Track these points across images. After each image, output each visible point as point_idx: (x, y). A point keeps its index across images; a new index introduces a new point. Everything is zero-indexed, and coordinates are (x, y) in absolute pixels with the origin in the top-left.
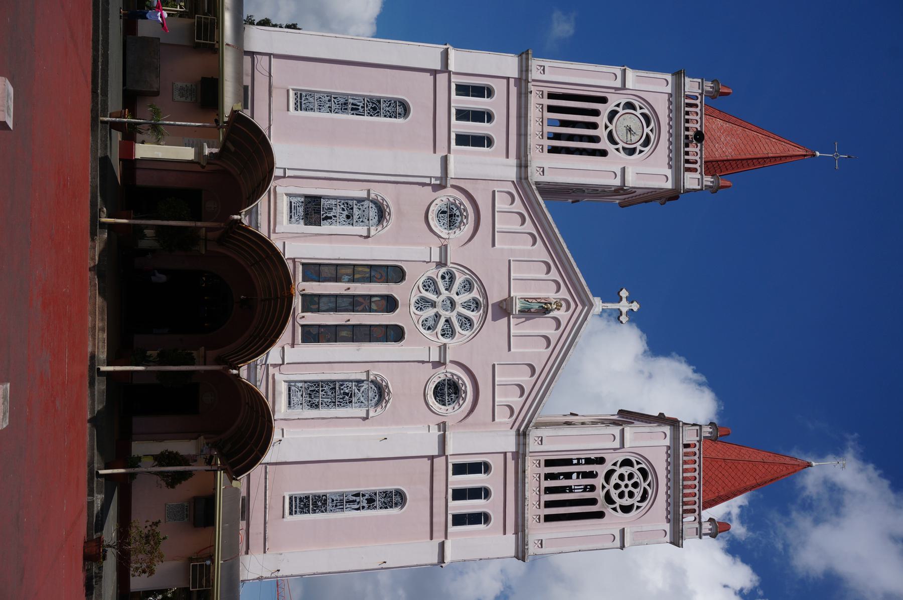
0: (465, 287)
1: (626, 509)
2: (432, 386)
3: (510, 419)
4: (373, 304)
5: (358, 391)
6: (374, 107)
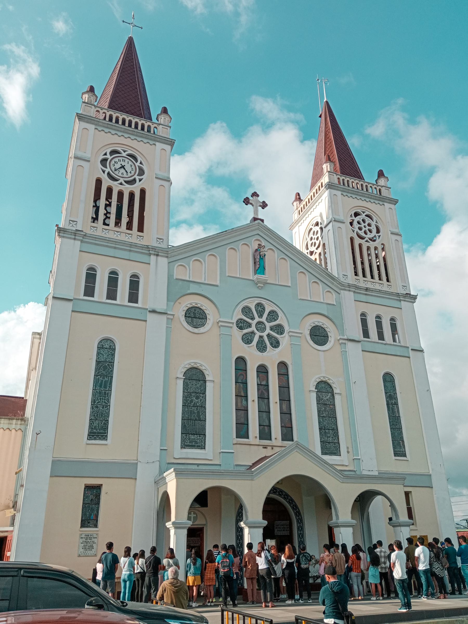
0: (246, 312)
3: (334, 294)
4: (262, 383)
5: (323, 401)
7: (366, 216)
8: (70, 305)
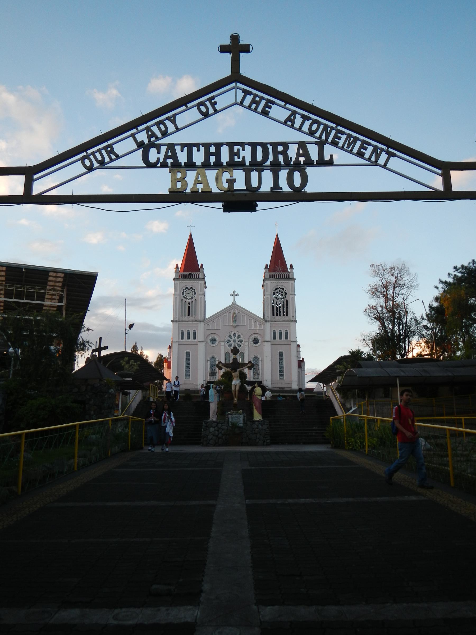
1: (286, 294)
6: (188, 360)
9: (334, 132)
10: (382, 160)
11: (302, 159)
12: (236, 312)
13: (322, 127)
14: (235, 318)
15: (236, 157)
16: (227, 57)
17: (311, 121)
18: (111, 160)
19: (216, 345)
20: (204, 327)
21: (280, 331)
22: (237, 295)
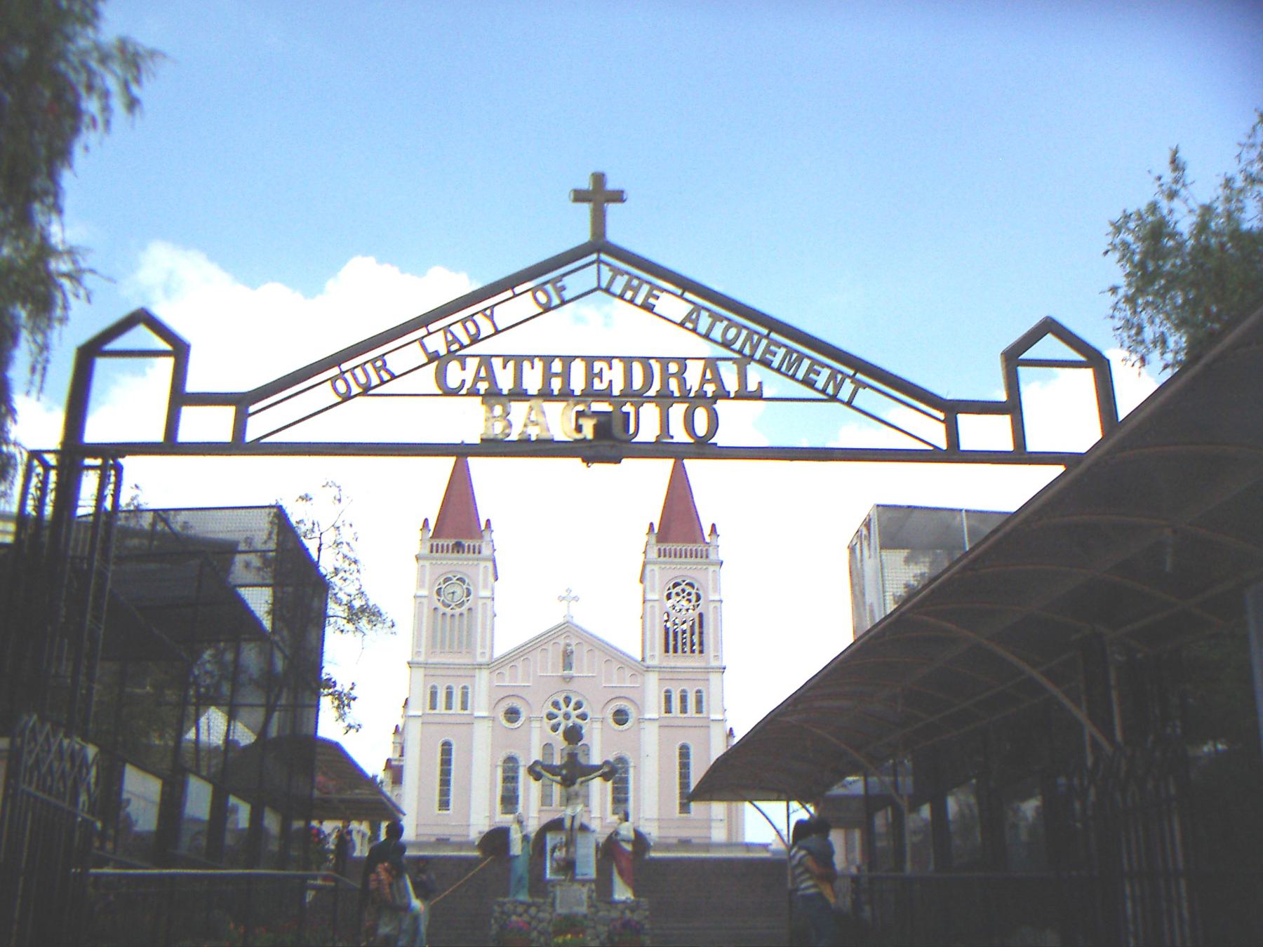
1: (698, 598)
2: (617, 727)
6: (446, 762)
7: (686, 584)
8: (420, 720)
9: (764, 342)
10: (845, 394)
11: (710, 389)
12: (574, 642)
13: (744, 332)
14: (567, 659)
15: (596, 381)
16: (586, 208)
17: (725, 323)
18: (383, 382)
19: (520, 725)
20: (491, 681)
21: (683, 691)
22: (576, 599)
